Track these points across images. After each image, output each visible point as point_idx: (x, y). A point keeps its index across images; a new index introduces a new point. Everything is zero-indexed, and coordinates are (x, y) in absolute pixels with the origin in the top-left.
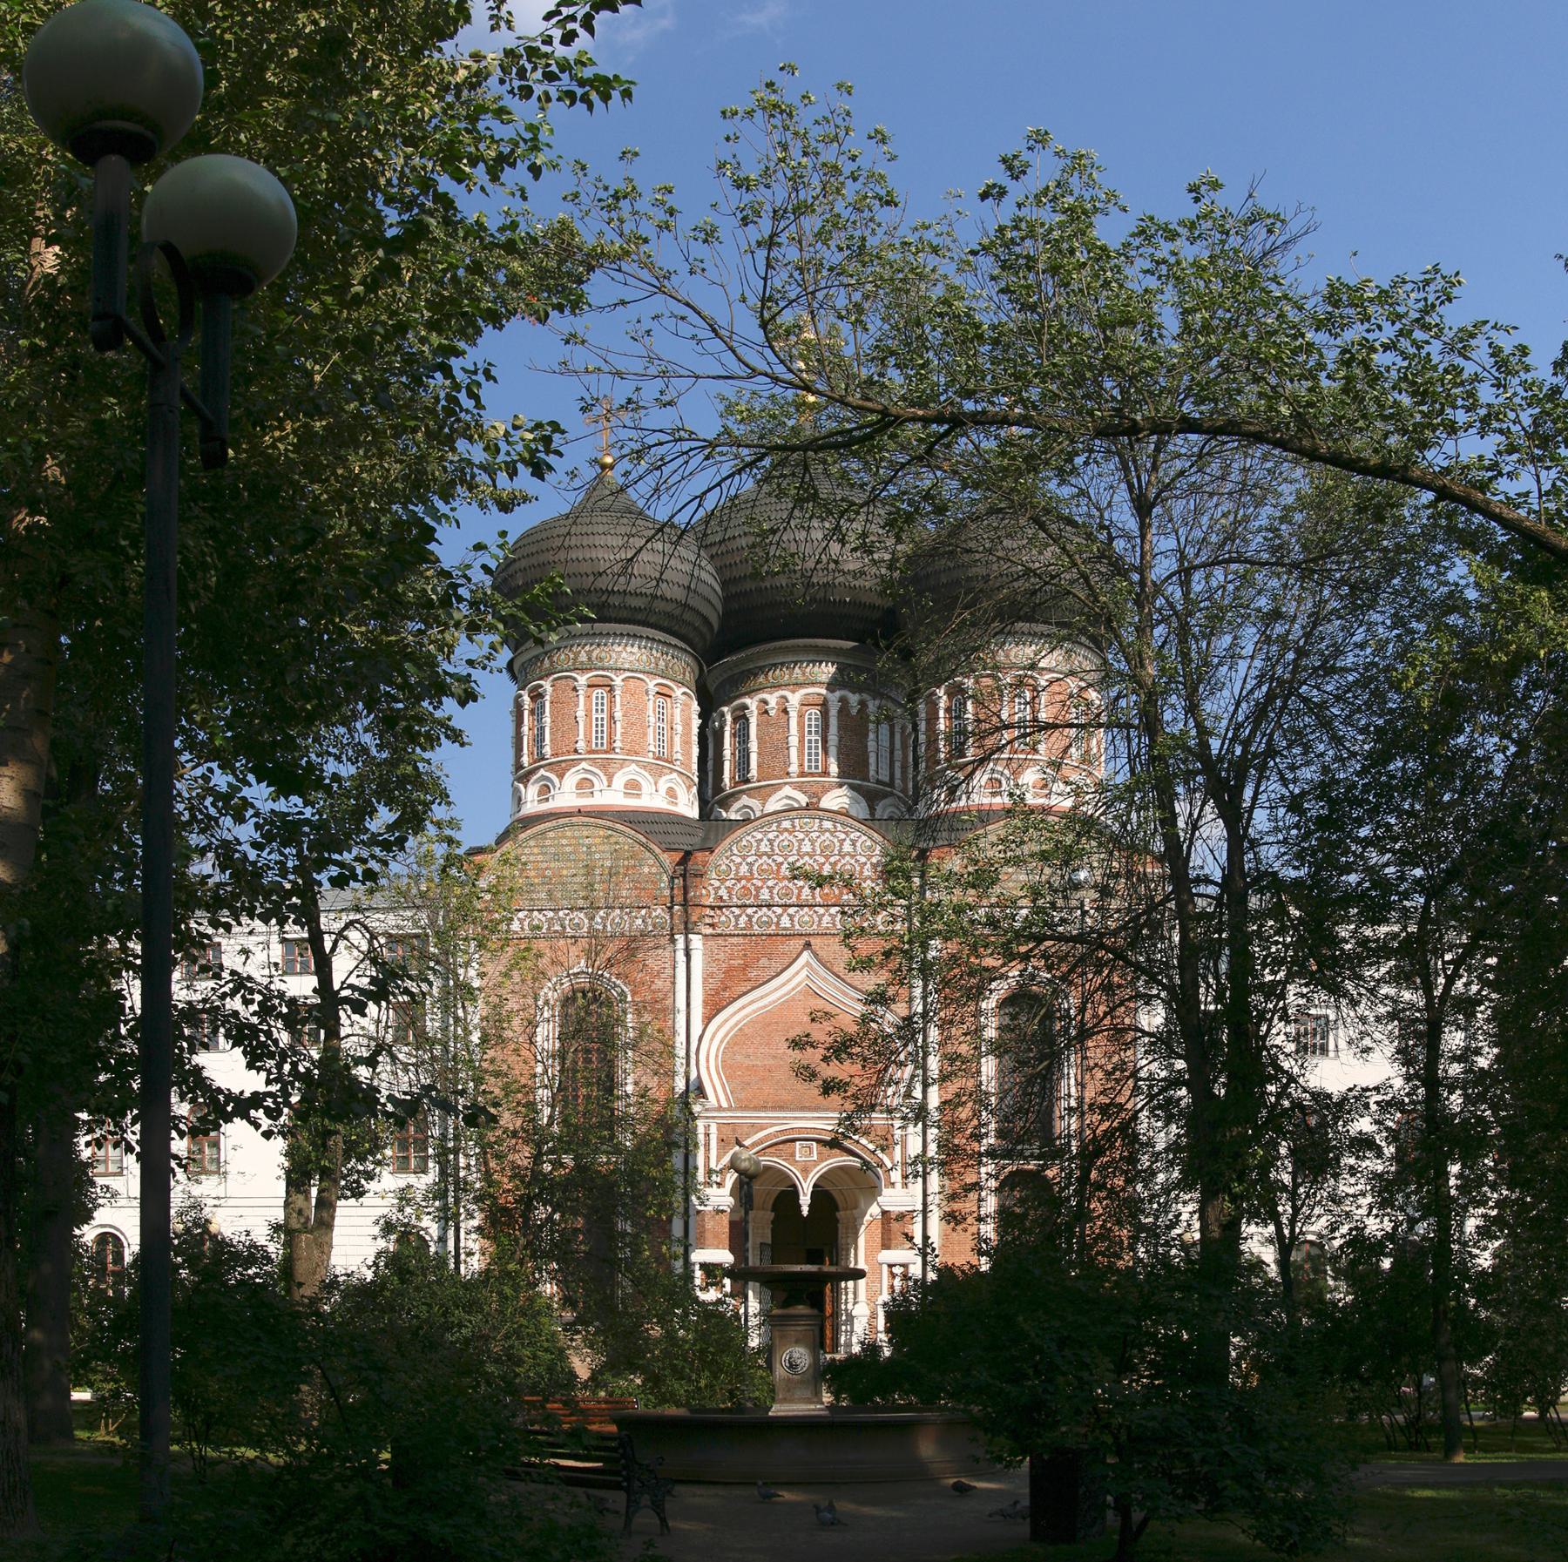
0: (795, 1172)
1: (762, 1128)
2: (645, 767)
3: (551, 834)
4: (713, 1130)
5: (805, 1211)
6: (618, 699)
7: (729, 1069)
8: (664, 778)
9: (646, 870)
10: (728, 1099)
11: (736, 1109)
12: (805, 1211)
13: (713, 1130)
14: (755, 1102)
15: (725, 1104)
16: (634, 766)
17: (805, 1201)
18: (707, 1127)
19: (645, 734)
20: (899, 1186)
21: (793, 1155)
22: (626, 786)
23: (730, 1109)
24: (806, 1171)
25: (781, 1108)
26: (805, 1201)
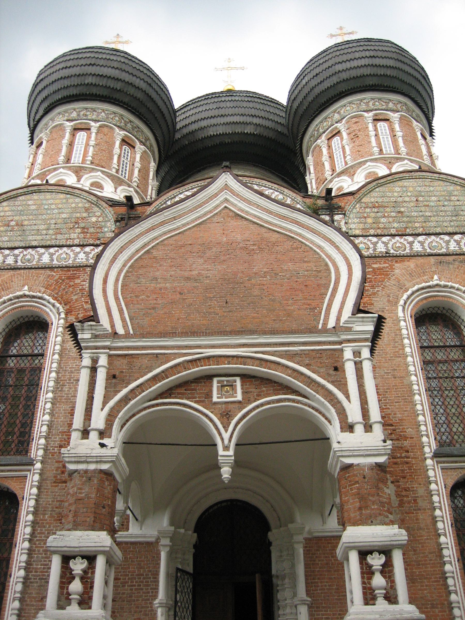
0: (211, 421)
1: (168, 358)
2: (108, 176)
3: (21, 198)
4: (103, 361)
5: (226, 472)
6: (93, 135)
7: (130, 289)
8: (122, 187)
9: (94, 219)
10: (125, 326)
11: (135, 336)
12: (226, 472)
13: (103, 361)
14: (160, 328)
15: (120, 331)
16: (99, 173)
17: (226, 454)
18: (95, 361)
19: (111, 158)
20: (359, 429)
21: (209, 395)
22: (92, 185)
23: (127, 336)
24: (226, 416)
25: (194, 333)
26: (226, 454)
